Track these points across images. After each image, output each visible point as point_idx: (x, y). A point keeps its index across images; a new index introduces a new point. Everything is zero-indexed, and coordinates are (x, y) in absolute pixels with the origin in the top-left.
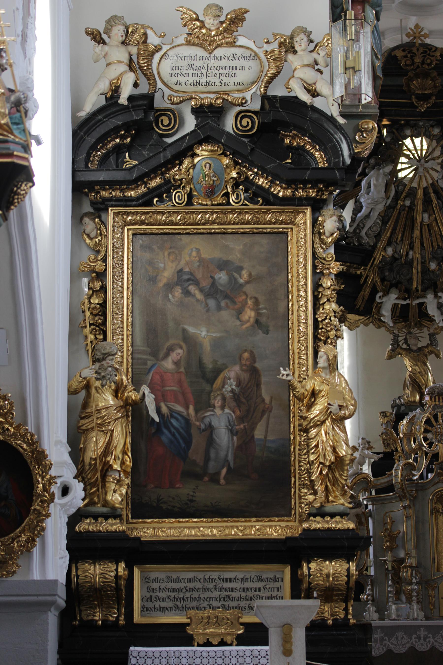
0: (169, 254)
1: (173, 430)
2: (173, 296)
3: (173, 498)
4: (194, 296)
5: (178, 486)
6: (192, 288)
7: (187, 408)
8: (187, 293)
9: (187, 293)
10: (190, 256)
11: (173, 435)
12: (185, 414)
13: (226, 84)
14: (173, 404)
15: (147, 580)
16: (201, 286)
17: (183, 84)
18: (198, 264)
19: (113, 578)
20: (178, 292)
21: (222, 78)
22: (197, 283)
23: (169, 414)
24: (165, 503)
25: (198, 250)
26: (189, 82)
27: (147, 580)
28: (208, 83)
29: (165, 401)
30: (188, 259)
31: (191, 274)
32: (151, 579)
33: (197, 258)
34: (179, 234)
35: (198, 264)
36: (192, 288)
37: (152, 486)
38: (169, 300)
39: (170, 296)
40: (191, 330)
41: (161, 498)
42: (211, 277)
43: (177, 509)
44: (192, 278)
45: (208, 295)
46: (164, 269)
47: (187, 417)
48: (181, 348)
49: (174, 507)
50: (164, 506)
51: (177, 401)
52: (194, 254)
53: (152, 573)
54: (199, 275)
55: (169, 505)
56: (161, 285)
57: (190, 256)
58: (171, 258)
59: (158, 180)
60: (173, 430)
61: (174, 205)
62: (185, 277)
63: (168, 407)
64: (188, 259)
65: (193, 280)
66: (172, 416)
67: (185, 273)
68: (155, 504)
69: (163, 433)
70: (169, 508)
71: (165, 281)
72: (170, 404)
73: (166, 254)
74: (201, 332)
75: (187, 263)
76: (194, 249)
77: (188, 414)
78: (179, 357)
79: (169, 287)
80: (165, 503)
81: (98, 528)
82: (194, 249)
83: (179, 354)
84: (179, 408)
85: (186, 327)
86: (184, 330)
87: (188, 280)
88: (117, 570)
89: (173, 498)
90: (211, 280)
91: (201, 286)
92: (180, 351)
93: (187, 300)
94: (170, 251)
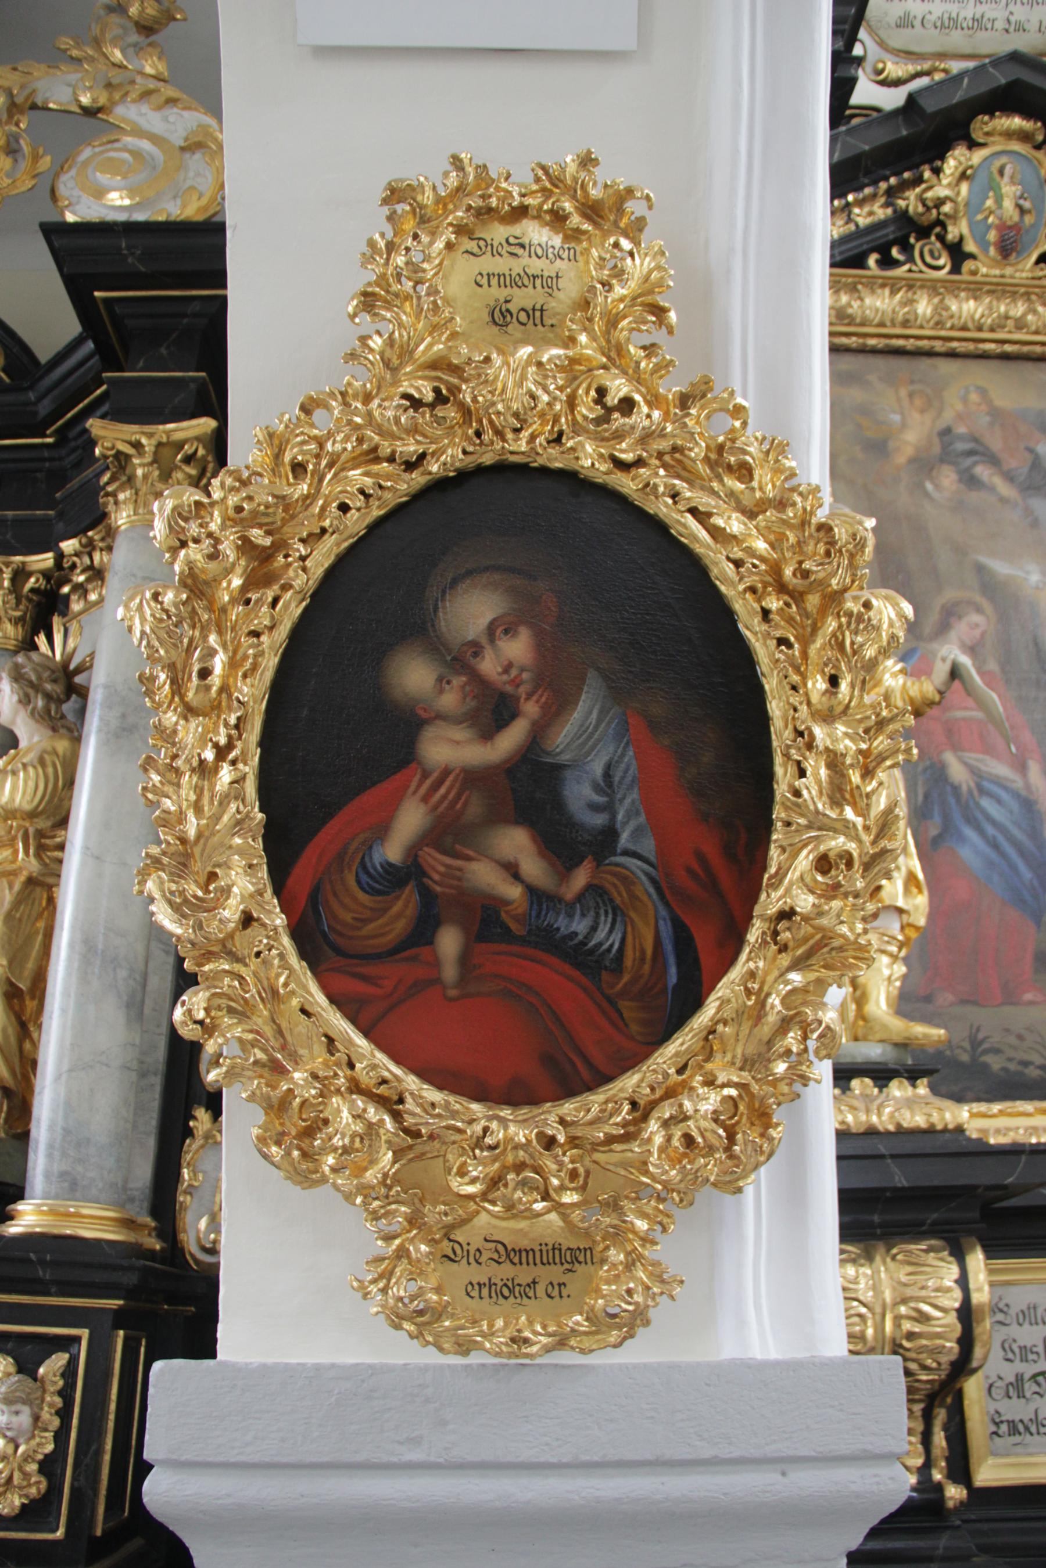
0: (911, 395)
1: (990, 830)
2: (937, 486)
3: (1020, 1037)
4: (992, 489)
5: (1028, 996)
6: (983, 471)
7: (1022, 767)
8: (971, 481)
9: (971, 481)
10: (965, 400)
11: (995, 846)
12: (1019, 784)
13: (1020, 28)
14: (981, 756)
15: (1000, 1317)
16: (1005, 468)
17: (917, 23)
18: (988, 419)
19: (952, 1318)
20: (948, 478)
21: (1011, 7)
22: (993, 460)
23: (972, 784)
24: (997, 1051)
25: (983, 392)
26: (933, 18)
27: (1000, 1317)
28: (978, 23)
29: (956, 748)
30: (960, 407)
31: (976, 440)
32: (1013, 1312)
33: (983, 407)
34: (930, 354)
35: (988, 419)
36: (983, 471)
37: (951, 998)
38: (927, 494)
39: (929, 486)
40: (1001, 568)
41: (980, 1036)
42: (1031, 450)
43: (1033, 1073)
44: (980, 449)
45: (1029, 488)
46: (904, 426)
47: (1024, 793)
48: (979, 610)
49: (1026, 1064)
50: (995, 1063)
51: (988, 750)
52: (974, 397)
53: (1013, 1289)
54: (995, 443)
55: (1010, 1060)
56: (901, 459)
57: (965, 400)
58: (918, 402)
59: (881, 212)
60: (990, 830)
61: (921, 272)
62: (961, 446)
63: (966, 764)
64: (960, 407)
65: (983, 454)
66: (982, 791)
67: (961, 438)
68: (965, 1058)
69: (962, 839)
70: (1012, 1067)
71: (909, 451)
72: (971, 757)
73: (903, 392)
74: (1028, 573)
75: (960, 417)
76: (972, 388)
77: (1028, 786)
78: (977, 633)
79: (924, 466)
80: (997, 1051)
81: (863, 1117)
82: (972, 388)
83: (977, 625)
84: (1001, 769)
85: (983, 559)
86: (980, 569)
87: (970, 453)
88: (963, 1282)
89: (1020, 1037)
90: (1029, 457)
91: (1005, 468)
92: (976, 618)
93: (974, 497)
94: (911, 388)
